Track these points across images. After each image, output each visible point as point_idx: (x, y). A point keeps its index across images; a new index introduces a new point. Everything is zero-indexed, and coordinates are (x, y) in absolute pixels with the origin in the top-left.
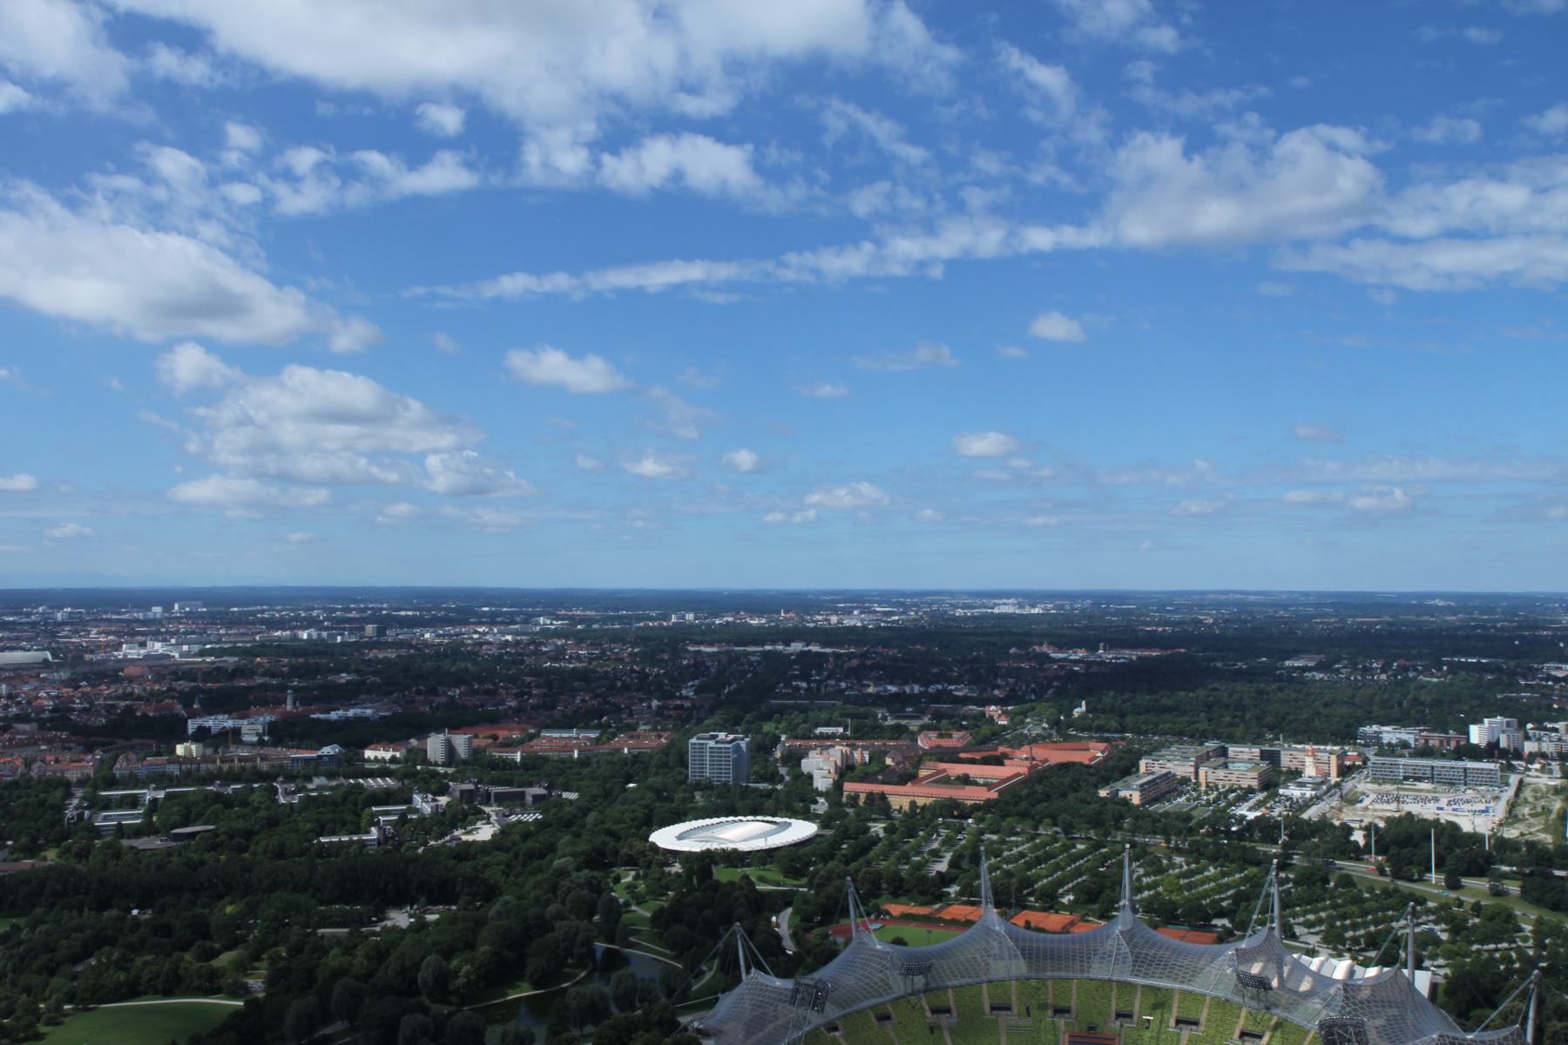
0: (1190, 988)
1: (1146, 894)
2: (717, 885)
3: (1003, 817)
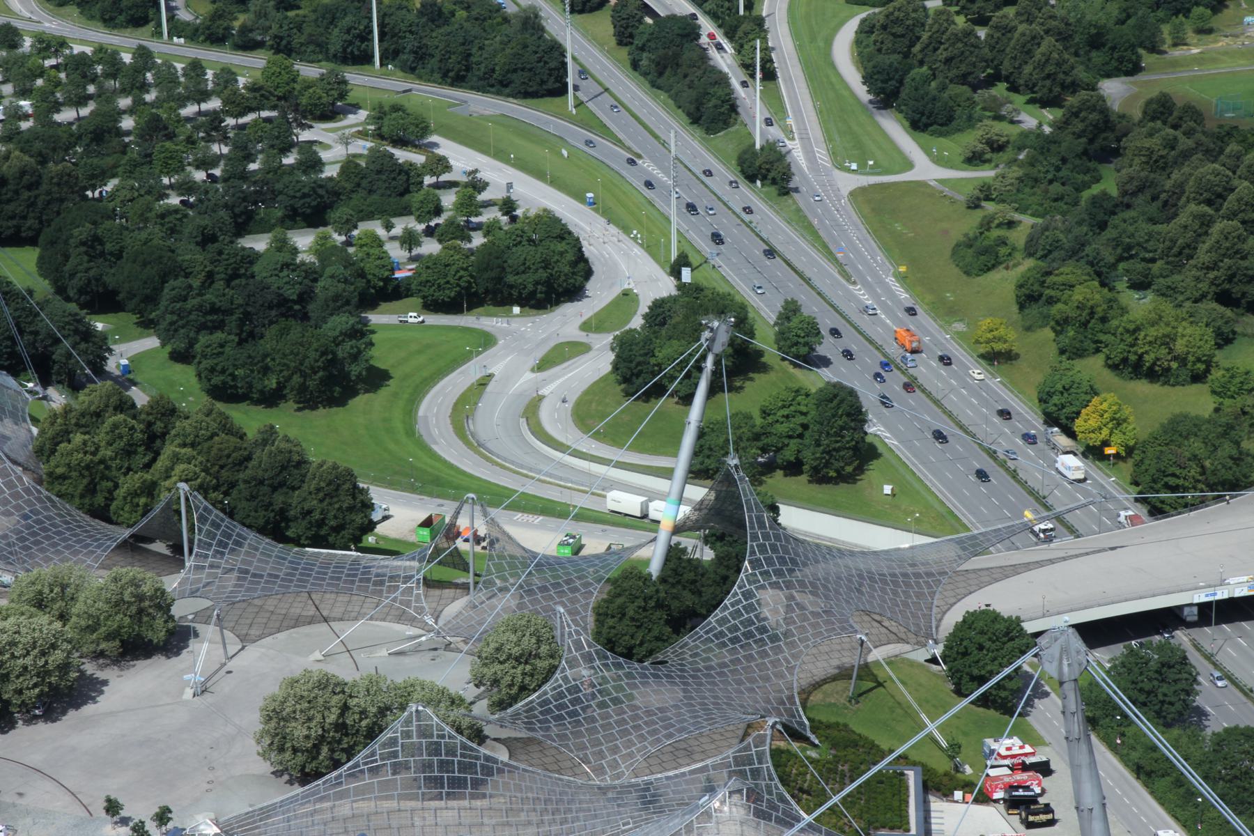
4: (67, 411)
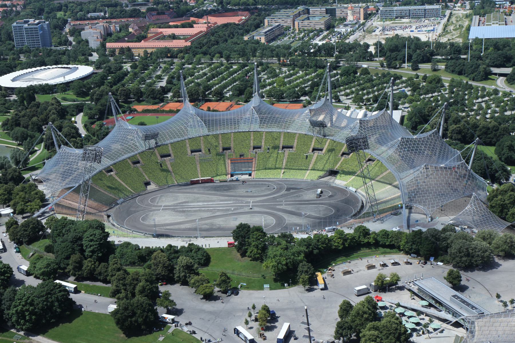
0: (288, 131)
1: (268, 88)
2: (38, 105)
3: (194, 56)
4: (497, 190)
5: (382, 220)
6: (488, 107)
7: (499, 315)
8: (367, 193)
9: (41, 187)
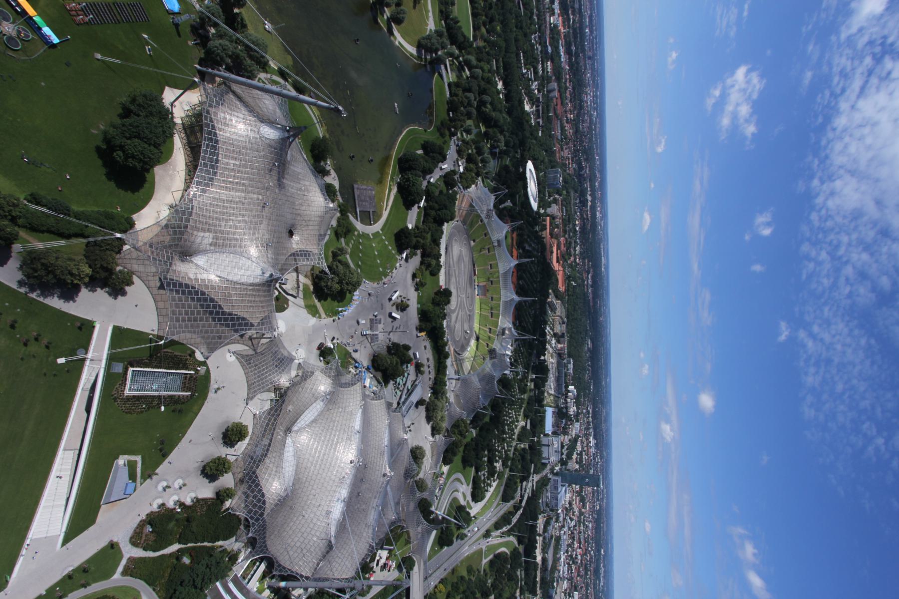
5: (452, 365)
6: (510, 418)
7: (404, 425)
8: (467, 358)
9: (473, 186)
